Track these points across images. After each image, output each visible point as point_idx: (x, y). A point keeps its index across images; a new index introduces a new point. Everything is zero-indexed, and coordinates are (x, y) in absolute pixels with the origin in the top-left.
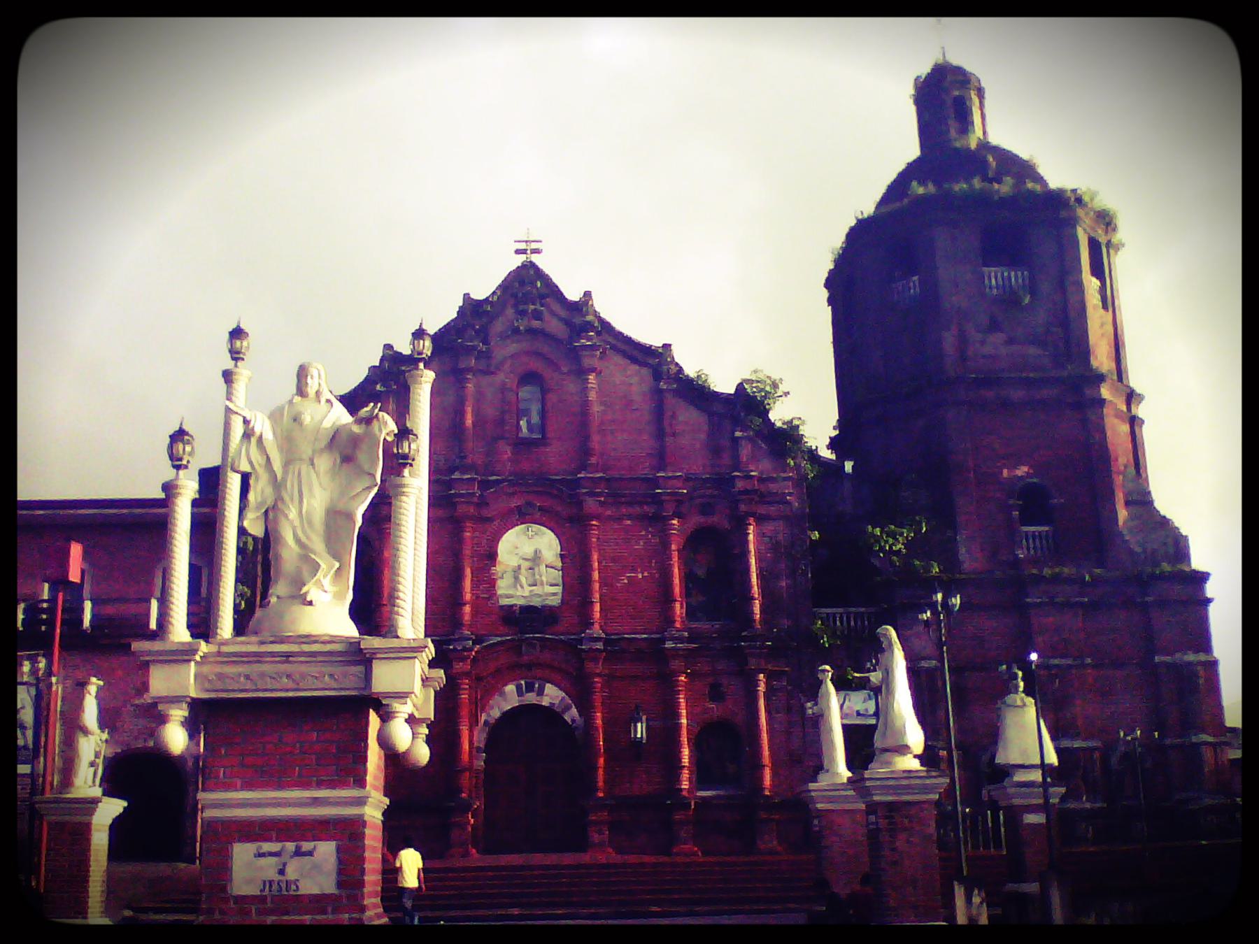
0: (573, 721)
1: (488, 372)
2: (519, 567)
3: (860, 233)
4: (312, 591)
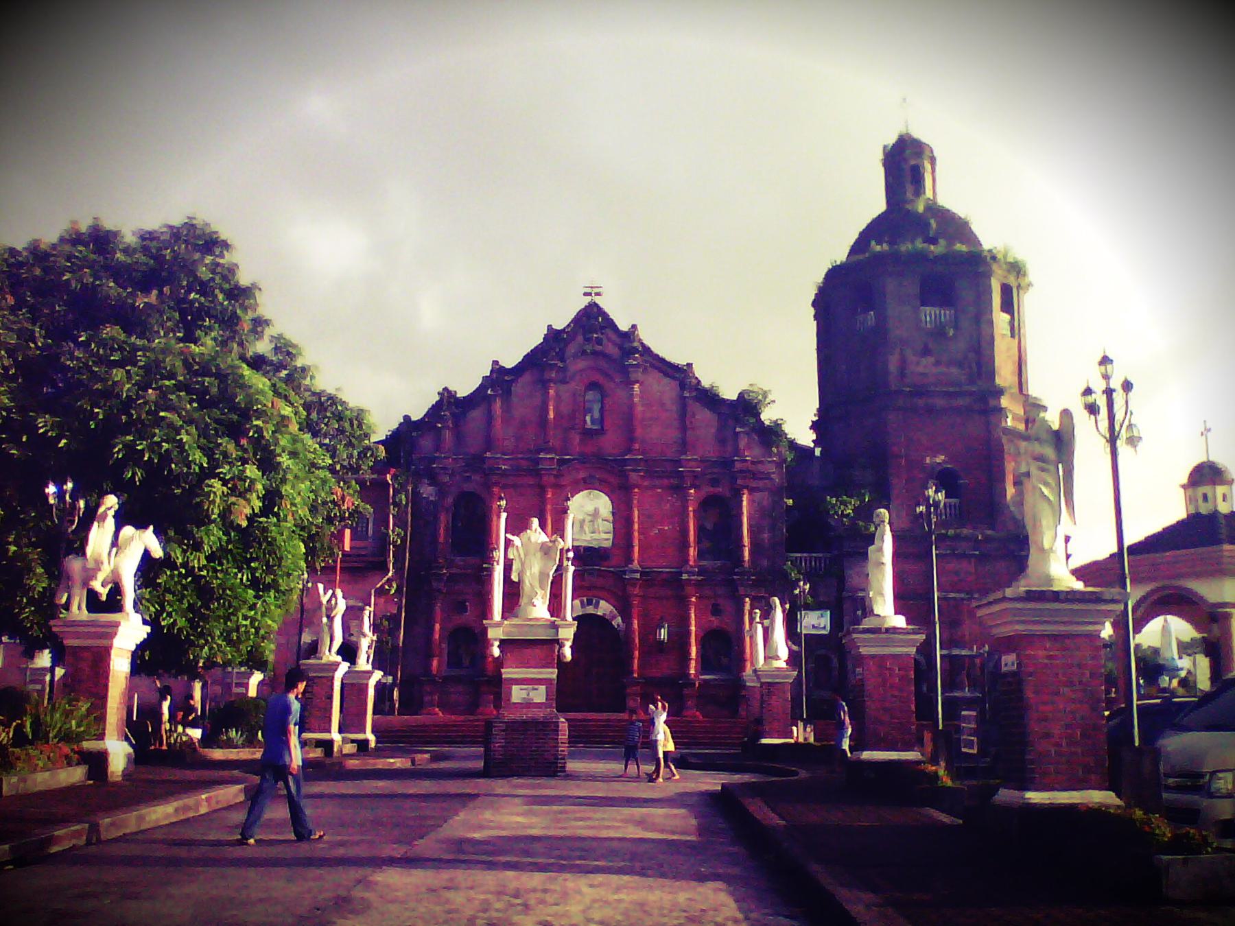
0: (618, 625)
1: (564, 382)
2: (584, 520)
3: (835, 275)
4: (535, 601)
